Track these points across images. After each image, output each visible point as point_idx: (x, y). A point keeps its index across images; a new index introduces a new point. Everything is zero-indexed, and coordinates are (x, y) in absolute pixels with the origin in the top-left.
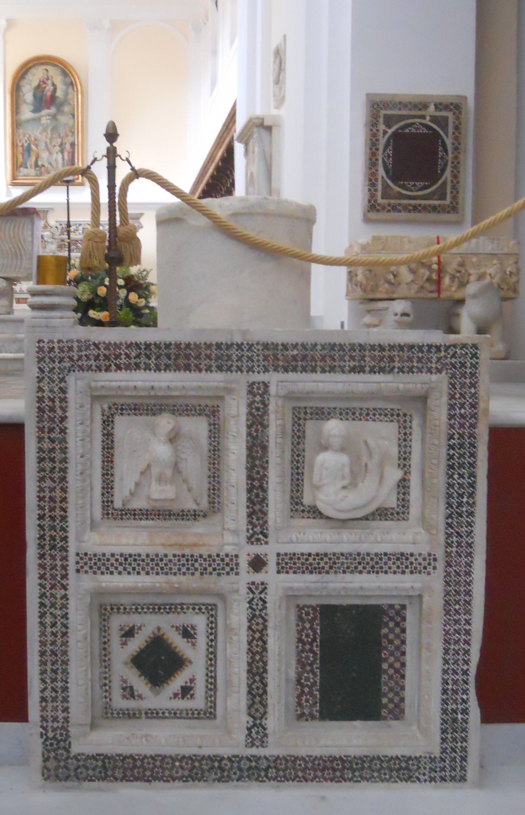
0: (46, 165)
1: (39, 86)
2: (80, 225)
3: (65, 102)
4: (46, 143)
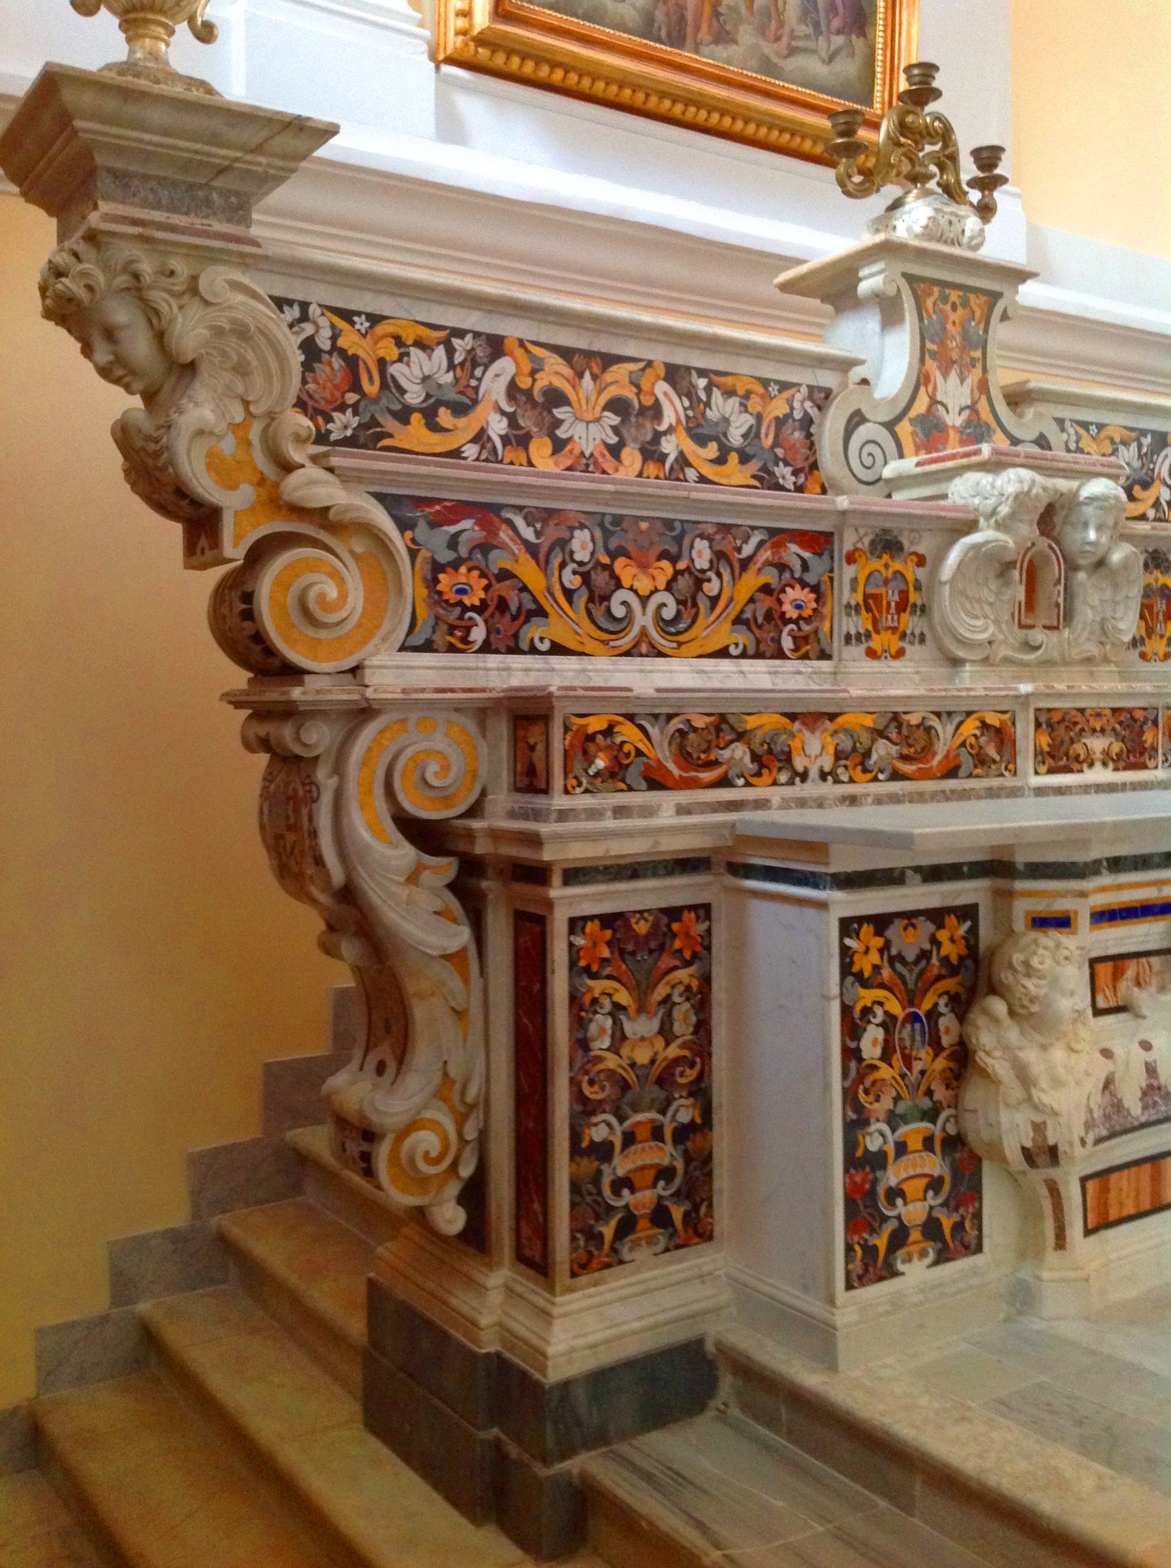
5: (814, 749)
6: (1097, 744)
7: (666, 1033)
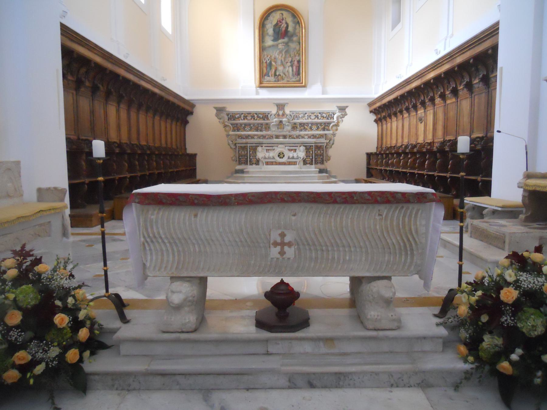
0: (282, 74)
5: (256, 137)
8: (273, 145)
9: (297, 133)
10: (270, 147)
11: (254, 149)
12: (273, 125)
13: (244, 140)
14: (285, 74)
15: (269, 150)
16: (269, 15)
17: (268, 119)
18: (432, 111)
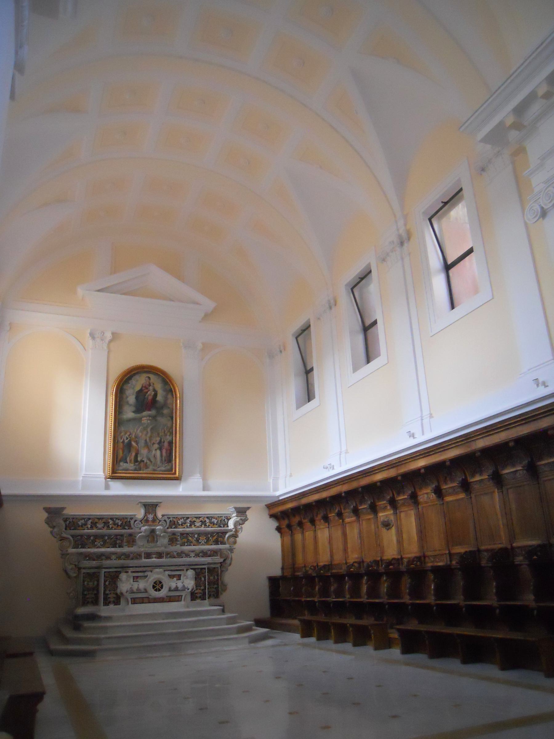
0: (145, 460)
1: (140, 391)
2: (188, 518)
3: (165, 405)
4: (146, 440)
5: (113, 557)
6: (154, 556)
7: (93, 584)
8: (144, 569)
9: (178, 548)
10: (140, 573)
11: (113, 578)
12: (142, 537)
13: (94, 562)
14: (149, 460)
15: (137, 577)
16: (130, 378)
17: (130, 527)
18: (412, 513)
